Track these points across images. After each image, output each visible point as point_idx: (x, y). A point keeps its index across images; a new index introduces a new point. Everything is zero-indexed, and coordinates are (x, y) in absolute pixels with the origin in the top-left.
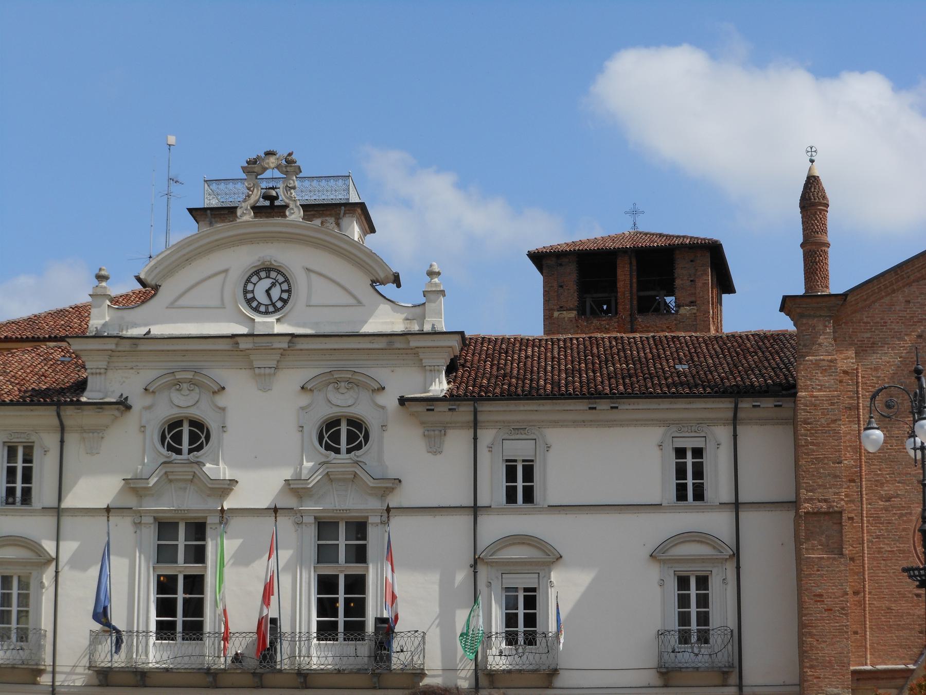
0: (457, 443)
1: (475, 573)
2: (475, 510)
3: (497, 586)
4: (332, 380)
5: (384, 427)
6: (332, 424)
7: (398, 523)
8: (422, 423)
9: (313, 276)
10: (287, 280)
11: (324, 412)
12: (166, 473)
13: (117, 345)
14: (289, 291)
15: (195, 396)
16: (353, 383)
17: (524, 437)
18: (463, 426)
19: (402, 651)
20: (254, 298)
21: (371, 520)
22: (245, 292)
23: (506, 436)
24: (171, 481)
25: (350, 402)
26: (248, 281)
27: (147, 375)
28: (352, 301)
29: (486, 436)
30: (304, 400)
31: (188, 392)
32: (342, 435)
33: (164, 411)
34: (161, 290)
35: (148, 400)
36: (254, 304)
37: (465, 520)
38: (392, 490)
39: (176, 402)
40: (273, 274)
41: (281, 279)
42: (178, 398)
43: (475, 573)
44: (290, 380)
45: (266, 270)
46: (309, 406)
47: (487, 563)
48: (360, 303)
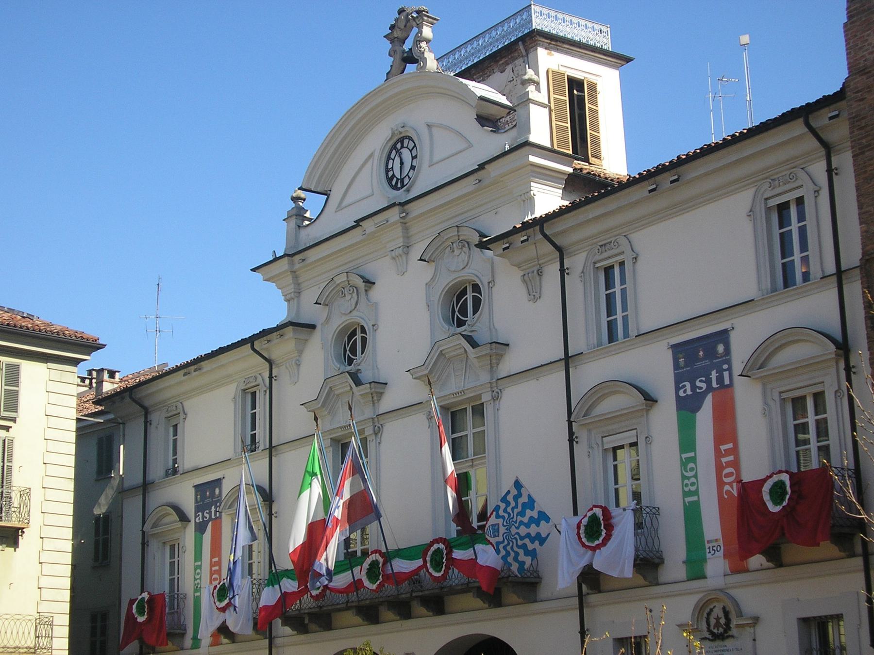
1: (571, 440)
2: (567, 360)
3: (598, 454)
5: (491, 283)
7: (512, 395)
8: (519, 266)
11: (446, 281)
14: (416, 157)
20: (394, 176)
22: (387, 171)
26: (389, 158)
29: (577, 262)
32: (462, 304)
33: (338, 322)
36: (394, 183)
38: (500, 357)
48: (470, 146)
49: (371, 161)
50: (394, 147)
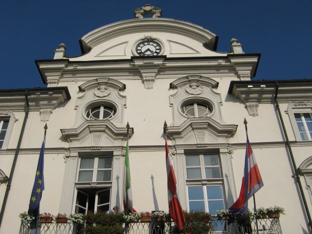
0: (266, 110)
2: (287, 144)
4: (188, 81)
6: (188, 104)
9: (171, 43)
10: (159, 45)
12: (88, 126)
13: (66, 66)
15: (108, 92)
16: (201, 82)
17: (304, 106)
18: (266, 101)
19: (265, 230)
21: (221, 151)
23: (294, 107)
24: (91, 132)
25: (199, 92)
26: (138, 45)
27: (81, 81)
28: (195, 52)
30: (173, 92)
31: (104, 90)
34: (92, 51)
35: (81, 94)
37: (283, 150)
39: (97, 95)
40: (151, 43)
41: (155, 45)
42: (98, 93)
43: (298, 178)
44: (162, 83)
45: (150, 40)
46: (175, 94)
47: (302, 174)
49: (125, 44)
50: (142, 43)
